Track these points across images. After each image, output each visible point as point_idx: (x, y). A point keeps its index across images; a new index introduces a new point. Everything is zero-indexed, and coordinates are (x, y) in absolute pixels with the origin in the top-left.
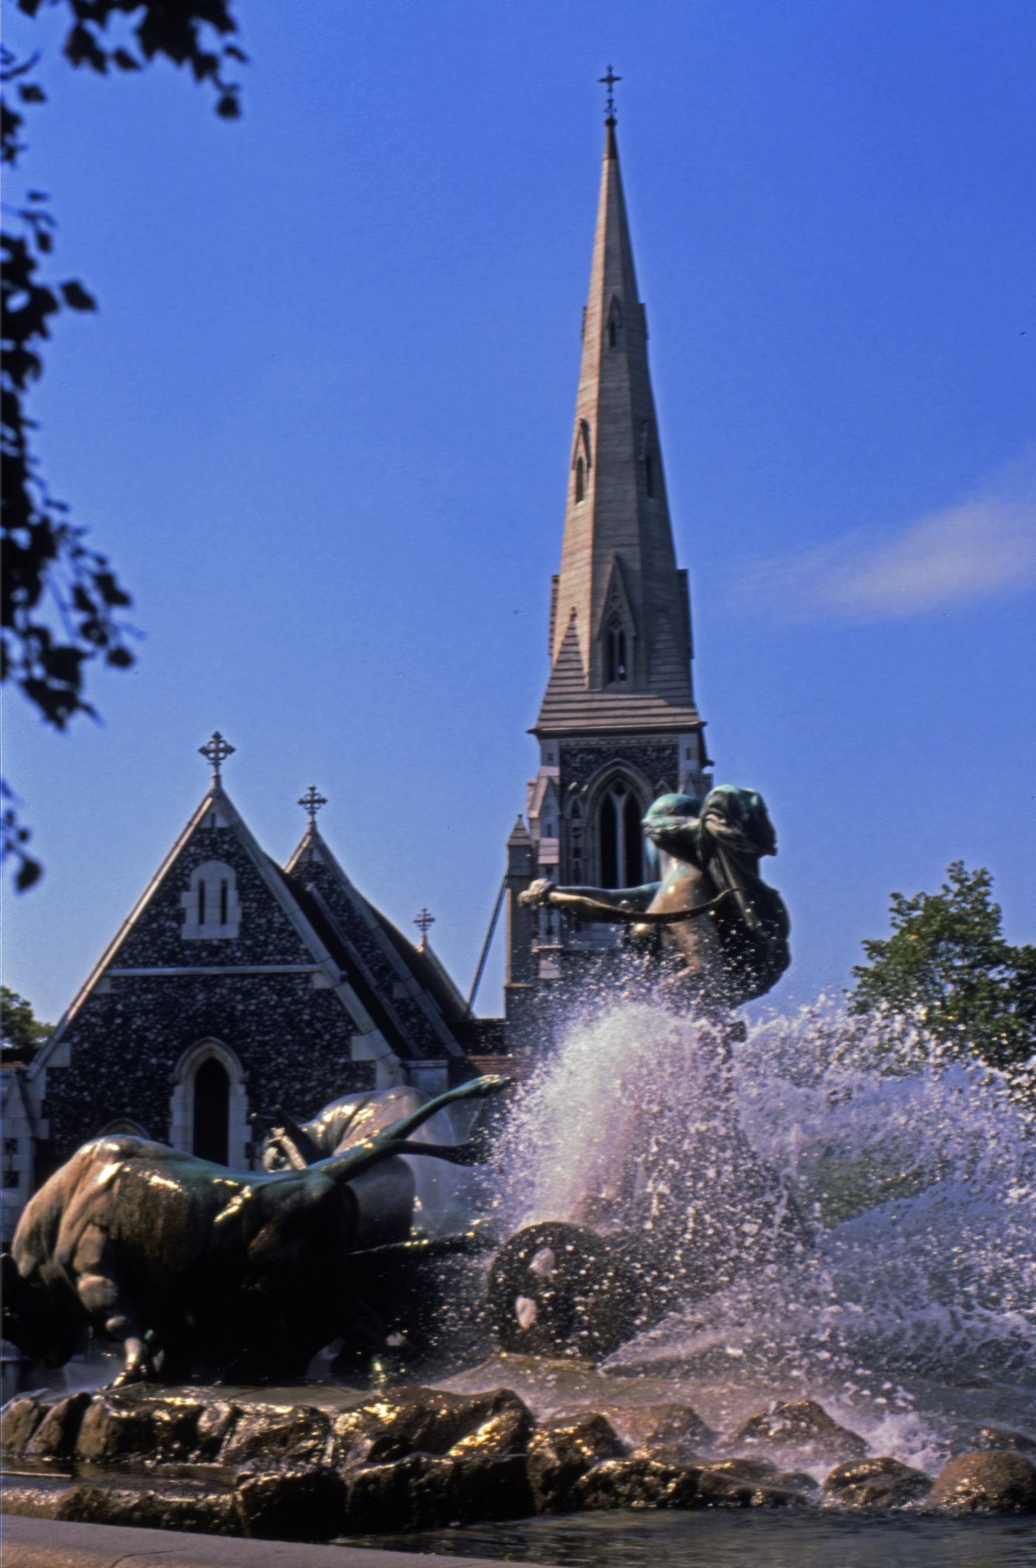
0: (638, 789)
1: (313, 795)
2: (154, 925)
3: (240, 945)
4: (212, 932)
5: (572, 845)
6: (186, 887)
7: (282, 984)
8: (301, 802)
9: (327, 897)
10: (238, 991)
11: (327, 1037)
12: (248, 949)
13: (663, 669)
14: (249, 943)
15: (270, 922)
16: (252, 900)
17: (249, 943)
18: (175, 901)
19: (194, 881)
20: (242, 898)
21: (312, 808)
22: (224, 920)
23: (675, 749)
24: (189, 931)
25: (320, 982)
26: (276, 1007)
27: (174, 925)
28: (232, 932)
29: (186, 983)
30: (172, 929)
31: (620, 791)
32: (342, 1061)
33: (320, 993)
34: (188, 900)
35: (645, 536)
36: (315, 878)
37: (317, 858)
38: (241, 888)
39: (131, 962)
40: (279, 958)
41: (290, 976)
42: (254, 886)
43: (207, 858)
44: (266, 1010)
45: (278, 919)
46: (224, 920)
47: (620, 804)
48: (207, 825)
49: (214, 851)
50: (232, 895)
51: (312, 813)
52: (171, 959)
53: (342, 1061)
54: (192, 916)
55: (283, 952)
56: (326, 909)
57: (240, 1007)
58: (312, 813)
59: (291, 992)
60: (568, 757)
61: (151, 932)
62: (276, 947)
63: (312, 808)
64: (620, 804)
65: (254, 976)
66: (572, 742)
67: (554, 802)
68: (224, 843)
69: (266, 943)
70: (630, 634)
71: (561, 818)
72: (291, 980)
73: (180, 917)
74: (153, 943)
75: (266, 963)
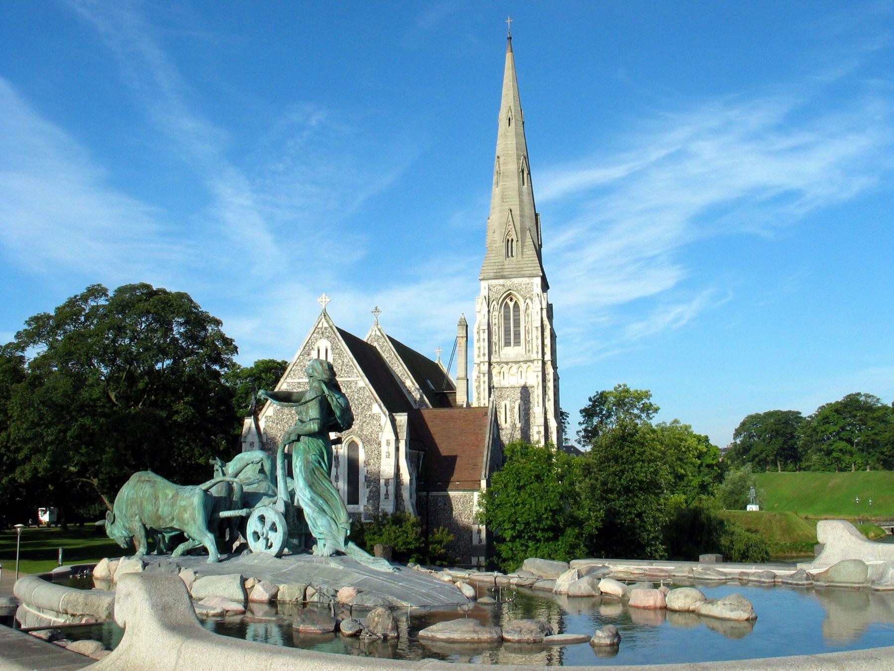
19: (316, 348)
23: (532, 284)
35: (521, 201)
38: (333, 349)
45: (346, 361)
47: (511, 304)
64: (511, 304)
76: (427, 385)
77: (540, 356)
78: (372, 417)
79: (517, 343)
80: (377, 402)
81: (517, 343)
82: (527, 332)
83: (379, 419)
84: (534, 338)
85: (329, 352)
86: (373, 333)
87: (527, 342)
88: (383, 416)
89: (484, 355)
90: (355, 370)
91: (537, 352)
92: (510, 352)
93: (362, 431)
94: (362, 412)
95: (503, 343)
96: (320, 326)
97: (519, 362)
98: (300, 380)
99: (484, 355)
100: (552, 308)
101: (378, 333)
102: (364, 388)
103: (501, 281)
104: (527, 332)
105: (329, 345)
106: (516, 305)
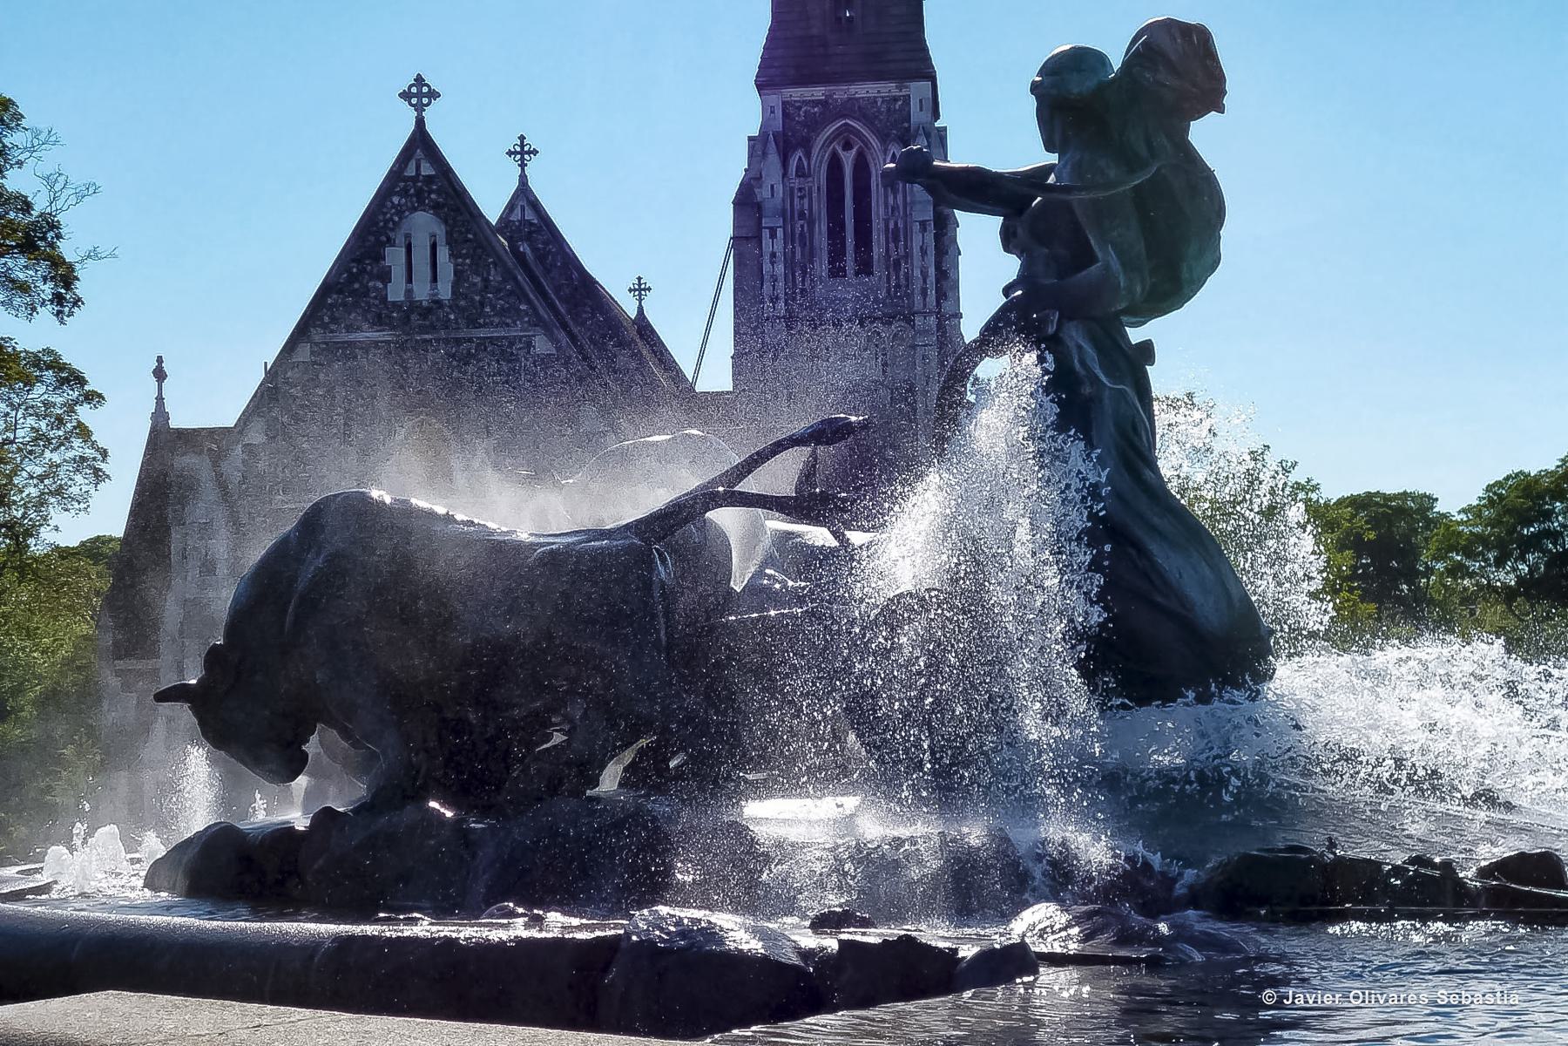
0: (866, 143)
1: (522, 146)
2: (356, 286)
3: (454, 306)
4: (422, 293)
6: (390, 242)
8: (510, 153)
12: (463, 310)
14: (462, 303)
15: (486, 280)
16: (465, 257)
17: (462, 303)
19: (400, 239)
20: (453, 255)
21: (522, 159)
22: (435, 279)
23: (907, 99)
28: (445, 291)
31: (847, 146)
34: (394, 258)
36: (529, 238)
37: (530, 215)
38: (450, 242)
39: (333, 327)
40: (496, 320)
43: (415, 209)
45: (495, 277)
46: (435, 279)
47: (848, 159)
48: (411, 171)
49: (421, 201)
50: (443, 254)
51: (523, 166)
54: (398, 273)
55: (503, 312)
58: (523, 166)
60: (791, 110)
62: (493, 308)
63: (522, 159)
64: (848, 159)
65: (470, 340)
66: (796, 93)
67: (774, 158)
68: (430, 192)
69: (482, 304)
71: (785, 175)
72: (511, 344)
73: (385, 277)
75: (481, 326)
79: (865, 267)
84: (916, 251)
85: (443, 254)
91: (924, 293)
95: (822, 266)
96: (411, 171)
101: (530, 215)
103: (818, 92)
104: (894, 236)
105: (440, 231)
106: (862, 166)
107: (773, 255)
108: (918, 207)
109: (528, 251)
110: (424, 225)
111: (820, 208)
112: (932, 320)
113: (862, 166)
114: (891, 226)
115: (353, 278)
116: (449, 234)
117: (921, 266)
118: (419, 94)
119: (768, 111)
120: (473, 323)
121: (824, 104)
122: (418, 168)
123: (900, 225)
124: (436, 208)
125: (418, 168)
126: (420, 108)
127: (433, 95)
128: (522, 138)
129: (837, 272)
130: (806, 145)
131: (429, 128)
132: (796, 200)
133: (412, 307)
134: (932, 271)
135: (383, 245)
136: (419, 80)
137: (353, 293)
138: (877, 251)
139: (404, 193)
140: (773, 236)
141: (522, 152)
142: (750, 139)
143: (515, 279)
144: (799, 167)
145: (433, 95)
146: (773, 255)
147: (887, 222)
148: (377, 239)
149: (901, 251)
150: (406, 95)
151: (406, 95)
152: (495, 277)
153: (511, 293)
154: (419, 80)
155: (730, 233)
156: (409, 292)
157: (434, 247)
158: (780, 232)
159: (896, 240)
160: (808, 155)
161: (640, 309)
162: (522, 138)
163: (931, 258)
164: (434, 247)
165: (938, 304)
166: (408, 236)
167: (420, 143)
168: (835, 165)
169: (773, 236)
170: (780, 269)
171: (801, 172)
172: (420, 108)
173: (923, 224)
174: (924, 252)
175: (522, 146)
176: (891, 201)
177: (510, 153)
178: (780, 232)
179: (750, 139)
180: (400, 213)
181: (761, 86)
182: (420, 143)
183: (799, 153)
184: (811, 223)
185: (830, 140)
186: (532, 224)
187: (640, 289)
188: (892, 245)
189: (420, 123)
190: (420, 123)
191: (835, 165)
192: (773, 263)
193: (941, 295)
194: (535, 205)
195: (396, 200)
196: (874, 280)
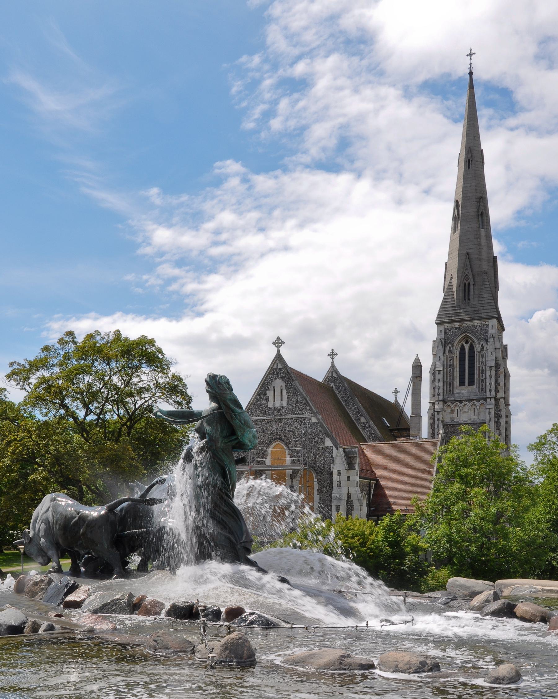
1: (333, 352)
3: (287, 408)
4: (278, 404)
5: (449, 363)
7: (301, 421)
8: (329, 355)
9: (338, 388)
10: (287, 424)
11: (316, 439)
12: (290, 409)
13: (485, 296)
18: (265, 394)
19: (271, 387)
21: (333, 357)
24: (270, 404)
25: (314, 420)
26: (299, 429)
27: (265, 402)
28: (285, 404)
29: (269, 422)
30: (264, 404)
31: (467, 342)
32: (321, 446)
33: (314, 424)
34: (270, 394)
36: (334, 382)
37: (334, 374)
38: (287, 389)
41: (304, 419)
42: (291, 388)
43: (276, 379)
44: (296, 430)
45: (300, 399)
47: (467, 347)
48: (275, 367)
49: (278, 376)
50: (284, 392)
51: (333, 359)
52: (265, 413)
53: (321, 446)
56: (337, 392)
57: (287, 429)
58: (333, 359)
59: (305, 423)
61: (258, 405)
62: (299, 408)
63: (333, 357)
64: (467, 347)
67: (441, 348)
69: (296, 407)
70: (472, 283)
71: (444, 353)
73: (267, 400)
74: (259, 409)
75: (296, 414)
76: (383, 422)
77: (493, 393)
78: (325, 449)
79: (471, 383)
80: (329, 436)
81: (471, 383)
82: (482, 372)
83: (331, 452)
85: (284, 392)
86: (330, 375)
87: (482, 381)
88: (334, 448)
89: (439, 394)
90: (308, 408)
91: (490, 391)
92: (465, 391)
93: (315, 462)
94: (315, 446)
95: (457, 382)
97: (472, 400)
98: (258, 418)
99: (439, 394)
100: (507, 348)
101: (334, 374)
102: (316, 423)
105: (283, 385)
106: (472, 348)
107: (439, 380)
108: (489, 362)
109: (334, 386)
110: (279, 384)
111: (457, 363)
112: (493, 401)
113: (472, 348)
114: (481, 368)
115: (258, 400)
116: (286, 386)
117: (490, 382)
118: (278, 343)
119: (439, 332)
120: (294, 413)
121: (459, 328)
122: (277, 366)
123: (484, 368)
124: (282, 378)
125: (277, 366)
126: (278, 347)
127: (283, 343)
128: (333, 350)
129: (462, 383)
130: (452, 343)
131: (281, 353)
132: (448, 361)
133: (274, 409)
134: (493, 383)
135: (266, 390)
136: (278, 338)
137: (258, 405)
138: (476, 376)
139: (273, 373)
140: (439, 374)
141: (333, 355)
142: (434, 341)
143: (306, 400)
144: (450, 350)
145: (283, 343)
146: (439, 380)
147: (479, 367)
148: (265, 388)
149: (484, 377)
150: (274, 343)
151: (274, 343)
152: (300, 399)
153: (305, 404)
154: (278, 338)
155: (411, 375)
156: (274, 404)
157: (282, 390)
158: (442, 372)
159: (482, 373)
160: (453, 346)
161: (396, 398)
162: (333, 350)
163: (493, 380)
164: (282, 390)
165: (496, 395)
166: (274, 387)
167: (279, 358)
168: (462, 349)
169: (439, 374)
170: (441, 384)
171: (450, 351)
172: (278, 347)
173: (490, 367)
174: (491, 377)
175: (333, 352)
176: (481, 360)
177: (329, 355)
178: (442, 372)
179: (434, 341)
180: (272, 380)
181: (437, 323)
182: (279, 358)
183: (450, 345)
184: (453, 369)
185: (460, 341)
186: (335, 377)
187: (396, 392)
188: (481, 375)
189: (279, 351)
190: (279, 351)
191: (462, 349)
192: (439, 382)
193: (497, 391)
194: (336, 371)
195: (270, 376)
196: (474, 386)
